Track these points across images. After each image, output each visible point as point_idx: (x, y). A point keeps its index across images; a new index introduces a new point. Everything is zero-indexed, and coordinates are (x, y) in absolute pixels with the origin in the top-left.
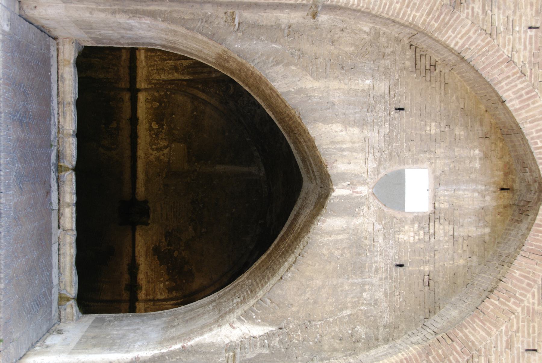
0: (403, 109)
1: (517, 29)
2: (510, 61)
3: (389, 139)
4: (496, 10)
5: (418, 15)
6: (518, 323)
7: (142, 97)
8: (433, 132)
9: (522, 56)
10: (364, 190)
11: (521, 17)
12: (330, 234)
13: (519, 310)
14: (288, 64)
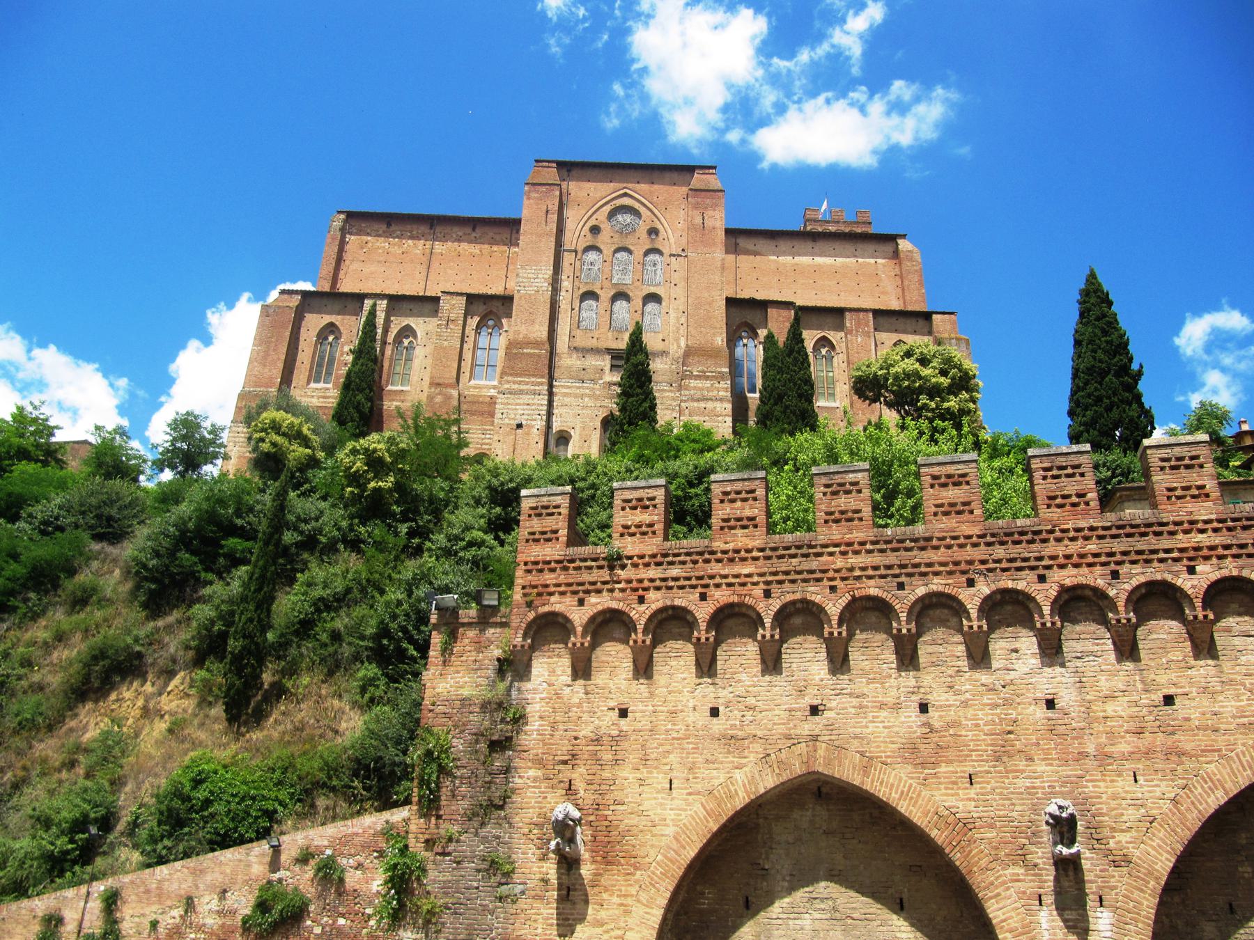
0: (1230, 905)
1: (1140, 795)
2: (1175, 801)
4: (1125, 818)
5: (1145, 903)
8: (1249, 869)
9: (1167, 788)
11: (1127, 792)
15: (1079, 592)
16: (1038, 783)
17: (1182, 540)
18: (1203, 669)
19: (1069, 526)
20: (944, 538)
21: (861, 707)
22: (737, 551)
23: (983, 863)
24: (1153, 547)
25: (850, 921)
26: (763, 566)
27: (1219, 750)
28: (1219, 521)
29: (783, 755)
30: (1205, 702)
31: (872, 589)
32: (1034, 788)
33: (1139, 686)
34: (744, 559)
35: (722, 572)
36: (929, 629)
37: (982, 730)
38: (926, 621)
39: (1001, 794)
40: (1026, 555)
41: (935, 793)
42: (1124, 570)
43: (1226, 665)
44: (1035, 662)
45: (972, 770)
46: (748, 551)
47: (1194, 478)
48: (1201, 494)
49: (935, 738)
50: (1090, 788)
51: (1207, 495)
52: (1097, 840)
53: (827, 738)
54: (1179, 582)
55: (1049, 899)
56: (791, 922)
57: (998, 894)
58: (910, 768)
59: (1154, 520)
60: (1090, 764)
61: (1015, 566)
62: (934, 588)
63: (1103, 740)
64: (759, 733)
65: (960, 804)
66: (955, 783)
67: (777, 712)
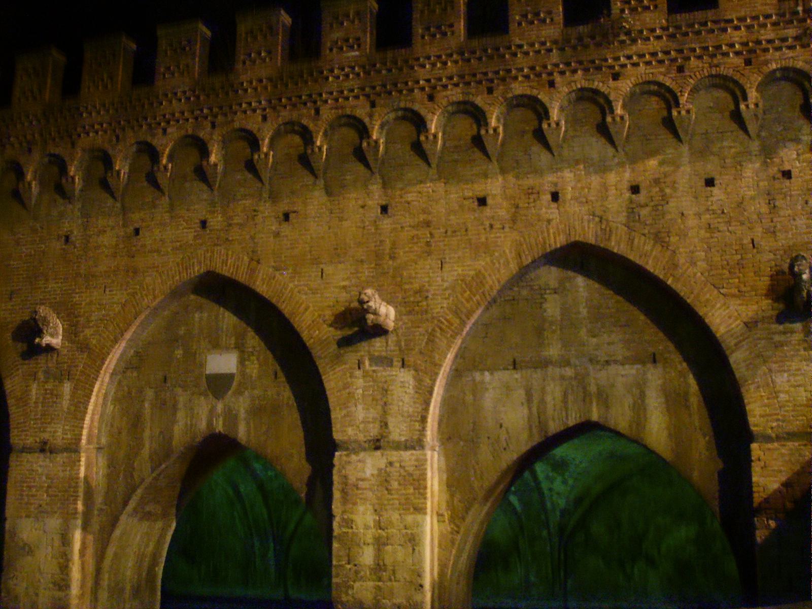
2: (124, 306)
3: (184, 387)
6: (301, 286)
7: (294, 594)
10: (220, 407)
13: (291, 285)
14: (134, 469)
32: (45, 299)
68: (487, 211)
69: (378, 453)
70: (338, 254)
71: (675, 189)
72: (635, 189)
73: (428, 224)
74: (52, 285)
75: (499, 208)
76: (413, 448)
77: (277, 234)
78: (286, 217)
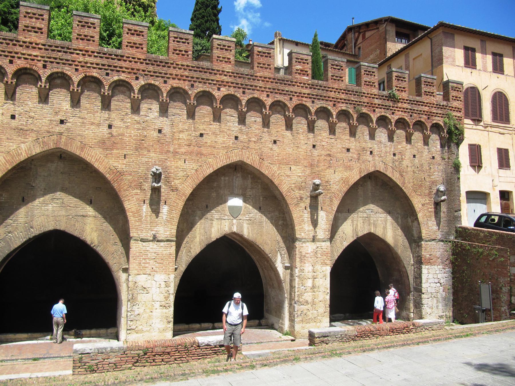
2: (196, 170)
4: (179, 175)
9: (195, 166)
12: (249, 233)
14: (191, 248)
15: (178, 90)
16: (150, 160)
17: (218, 77)
18: (215, 126)
19: (180, 63)
20: (129, 57)
21: (83, 123)
22: (31, 43)
23: (125, 188)
24: (208, 78)
25: (68, 208)
26: (43, 53)
27: (214, 154)
28: (232, 73)
29: (45, 140)
30: (213, 137)
31: (95, 73)
33: (193, 129)
34: (34, 48)
35: (22, 52)
36: (117, 95)
37: (132, 138)
38: (116, 91)
39: (136, 163)
40: (161, 71)
41: (110, 160)
42: (196, 84)
43: (223, 125)
44: (157, 114)
45: (126, 153)
46: (36, 44)
47: (227, 55)
48: (228, 61)
49: (113, 139)
50: (169, 164)
51: (230, 62)
52: (168, 181)
53: (66, 134)
54: (214, 93)
55: (147, 202)
56: (43, 208)
57: (129, 199)
58: (101, 150)
59: (210, 68)
60: (170, 155)
61: (156, 75)
62: (122, 78)
63: (177, 147)
64: (35, 129)
65: (120, 166)
66: (118, 157)
67: (44, 121)
68: (350, 154)
69: (313, 243)
70: (297, 162)
71: (405, 157)
72: (394, 155)
73: (329, 155)
74: (152, 154)
75: (353, 154)
76: (325, 241)
77: (271, 149)
78: (275, 142)
